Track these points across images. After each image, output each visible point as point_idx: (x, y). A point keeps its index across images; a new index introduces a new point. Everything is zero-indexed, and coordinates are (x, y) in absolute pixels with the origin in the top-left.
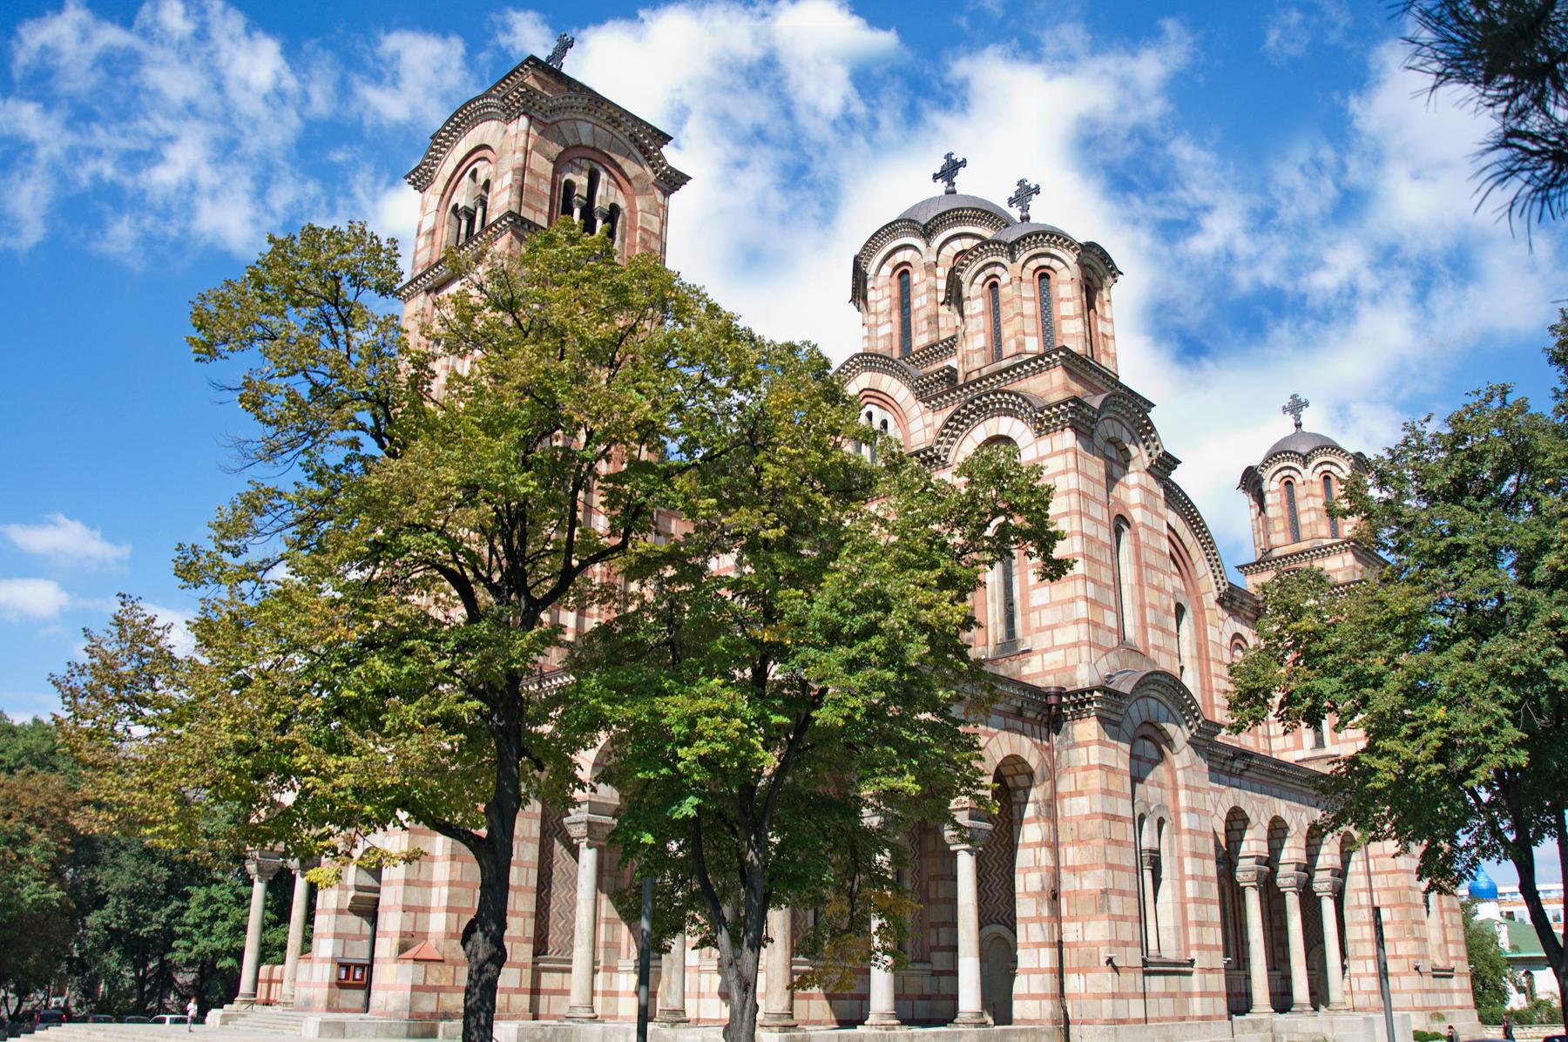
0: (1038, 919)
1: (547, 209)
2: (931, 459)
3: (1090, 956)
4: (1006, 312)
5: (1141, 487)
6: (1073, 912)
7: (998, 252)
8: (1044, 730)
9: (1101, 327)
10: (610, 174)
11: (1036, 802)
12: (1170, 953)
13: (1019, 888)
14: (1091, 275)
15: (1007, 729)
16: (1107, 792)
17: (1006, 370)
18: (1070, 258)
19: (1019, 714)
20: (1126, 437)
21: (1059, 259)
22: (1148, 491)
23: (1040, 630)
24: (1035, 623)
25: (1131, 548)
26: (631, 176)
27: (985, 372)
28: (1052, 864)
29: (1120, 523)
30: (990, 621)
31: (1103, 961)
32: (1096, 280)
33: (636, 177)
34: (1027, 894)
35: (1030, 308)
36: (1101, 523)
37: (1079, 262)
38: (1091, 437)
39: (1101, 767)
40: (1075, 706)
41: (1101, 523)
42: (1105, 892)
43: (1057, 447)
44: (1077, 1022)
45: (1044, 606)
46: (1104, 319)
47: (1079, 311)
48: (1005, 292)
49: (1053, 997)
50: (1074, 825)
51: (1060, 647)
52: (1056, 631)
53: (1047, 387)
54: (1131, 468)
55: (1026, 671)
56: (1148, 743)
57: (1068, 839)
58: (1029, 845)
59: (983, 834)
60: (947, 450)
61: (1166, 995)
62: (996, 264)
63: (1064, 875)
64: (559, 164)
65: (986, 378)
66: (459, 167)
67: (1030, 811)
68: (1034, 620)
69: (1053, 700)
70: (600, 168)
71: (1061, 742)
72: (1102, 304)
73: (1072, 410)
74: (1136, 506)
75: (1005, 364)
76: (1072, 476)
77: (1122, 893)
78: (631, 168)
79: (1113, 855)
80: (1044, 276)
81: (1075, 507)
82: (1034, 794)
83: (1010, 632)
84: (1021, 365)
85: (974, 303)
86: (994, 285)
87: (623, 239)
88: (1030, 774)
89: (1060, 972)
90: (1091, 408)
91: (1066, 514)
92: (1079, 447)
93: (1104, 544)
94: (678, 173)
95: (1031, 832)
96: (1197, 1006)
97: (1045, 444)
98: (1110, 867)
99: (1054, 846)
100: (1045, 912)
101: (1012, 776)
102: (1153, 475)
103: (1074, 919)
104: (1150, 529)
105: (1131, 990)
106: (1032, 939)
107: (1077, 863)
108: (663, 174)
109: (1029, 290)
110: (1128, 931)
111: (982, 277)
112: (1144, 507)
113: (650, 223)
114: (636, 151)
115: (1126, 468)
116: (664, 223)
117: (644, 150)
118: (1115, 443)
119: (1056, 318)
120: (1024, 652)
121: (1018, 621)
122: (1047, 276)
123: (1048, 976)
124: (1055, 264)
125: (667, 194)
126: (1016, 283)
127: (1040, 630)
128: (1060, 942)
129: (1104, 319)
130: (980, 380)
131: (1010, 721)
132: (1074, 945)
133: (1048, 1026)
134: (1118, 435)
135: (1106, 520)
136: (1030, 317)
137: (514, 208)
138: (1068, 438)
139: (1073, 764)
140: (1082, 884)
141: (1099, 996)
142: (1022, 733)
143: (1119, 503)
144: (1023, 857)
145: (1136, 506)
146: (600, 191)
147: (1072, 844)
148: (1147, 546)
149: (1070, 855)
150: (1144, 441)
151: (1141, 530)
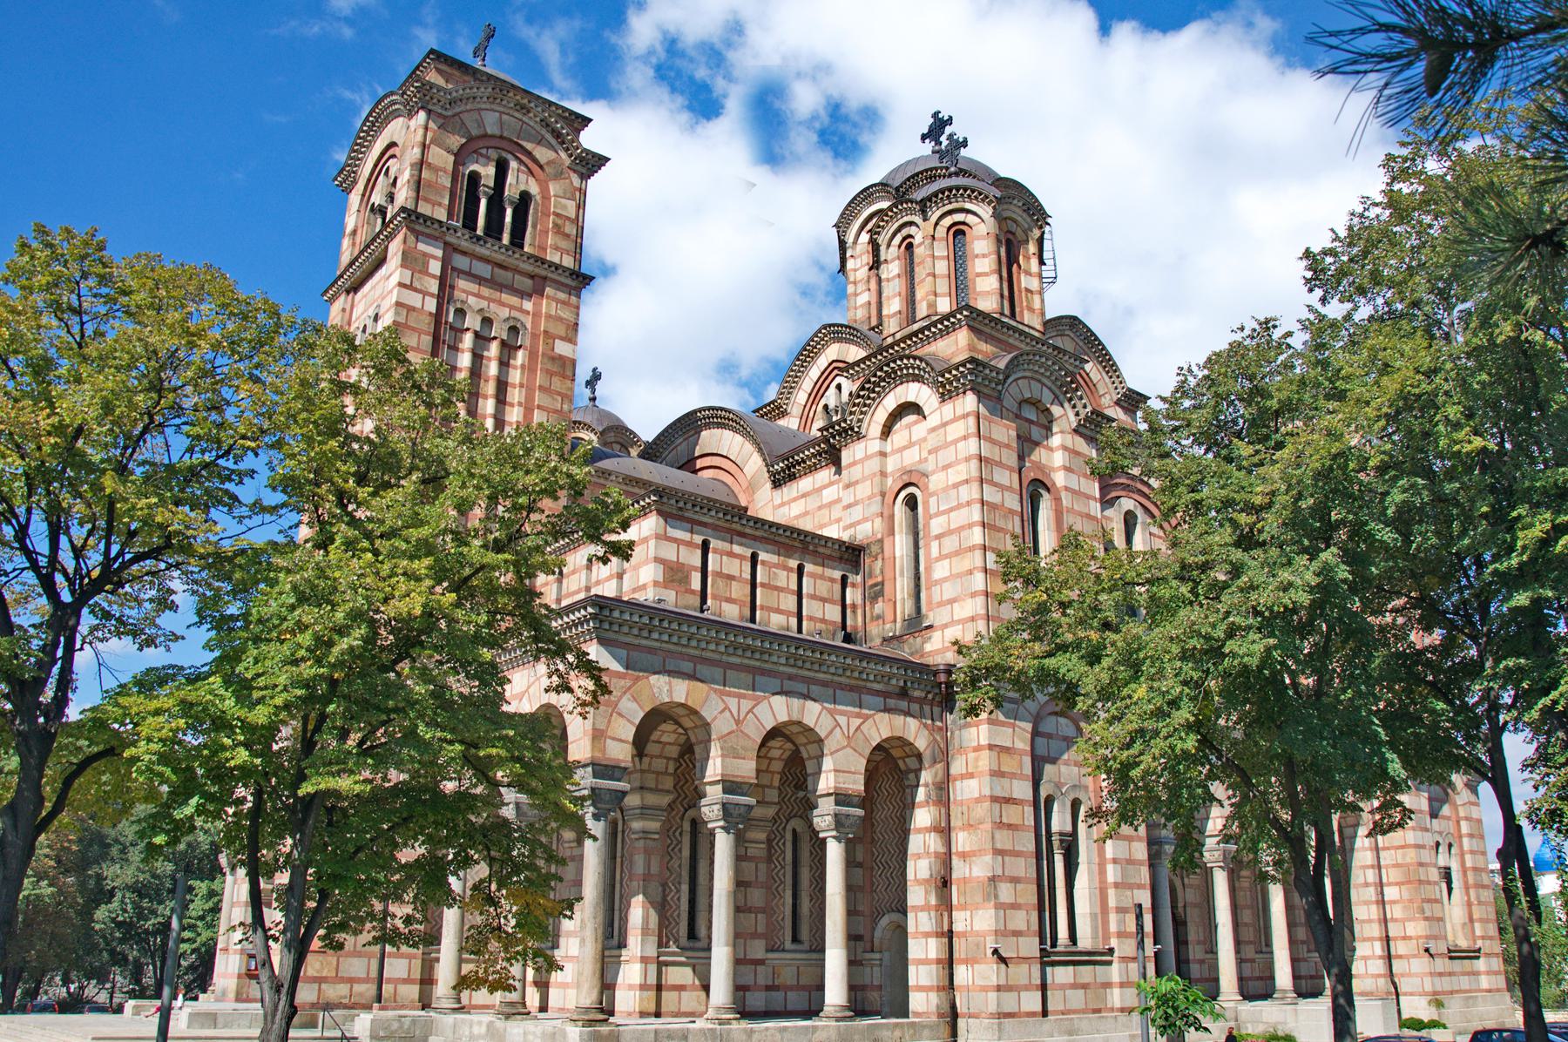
1: (446, 202)
2: (845, 430)
3: (977, 945)
4: (920, 272)
5: (1065, 448)
6: (962, 901)
7: (911, 211)
8: (936, 710)
9: (1025, 282)
10: (521, 161)
11: (926, 785)
12: (1085, 942)
13: (910, 875)
14: (1013, 227)
15: (887, 710)
16: (997, 774)
17: (915, 334)
18: (985, 211)
19: (903, 693)
20: (1047, 397)
21: (975, 214)
22: (1072, 452)
23: (941, 604)
24: (936, 598)
25: (1052, 514)
26: (543, 161)
27: (898, 336)
28: (942, 850)
29: (1035, 490)
30: (899, 597)
31: (989, 952)
32: (1019, 233)
33: (548, 163)
34: (918, 882)
35: (942, 267)
36: (1009, 489)
37: (994, 215)
38: (999, 399)
39: (991, 747)
41: (1009, 489)
42: (993, 879)
43: (959, 412)
45: (945, 580)
46: (1028, 273)
47: (994, 266)
48: (919, 252)
49: (939, 989)
51: (960, 622)
52: (956, 605)
53: (953, 349)
54: (1055, 429)
55: (928, 647)
56: (1062, 720)
57: (959, 823)
58: (919, 831)
59: (852, 819)
60: (860, 421)
61: (1075, 986)
62: (911, 223)
63: (955, 861)
64: (460, 156)
65: (897, 343)
66: (376, 166)
67: (921, 794)
69: (942, 678)
70: (509, 157)
71: (954, 722)
72: (1028, 258)
73: (971, 372)
74: (1059, 469)
75: (916, 327)
76: (973, 442)
77: (1015, 880)
78: (543, 154)
79: (1004, 840)
80: (958, 231)
81: (975, 473)
82: (926, 776)
83: (918, 609)
84: (928, 328)
85: (891, 266)
86: (910, 247)
87: (534, 226)
88: (919, 756)
89: (949, 963)
90: (993, 368)
91: (967, 482)
92: (982, 410)
93: (1011, 511)
94: (594, 155)
95: (923, 817)
96: (1116, 997)
97: (948, 410)
98: (998, 852)
99: (944, 831)
100: (933, 901)
101: (903, 758)
102: (1081, 435)
103: (963, 907)
104: (1075, 493)
105: (1025, 981)
106: (921, 929)
108: (581, 159)
109: (941, 250)
110: (1025, 920)
111: (898, 238)
112: (1068, 469)
113: (565, 207)
114: (549, 136)
115: (1049, 429)
116: (581, 206)
117: (557, 135)
118: (1035, 403)
119: (970, 276)
120: (928, 627)
121: (923, 595)
122: (963, 233)
123: (934, 967)
124: (970, 219)
125: (585, 177)
126: (928, 242)
127: (941, 604)
128: (951, 931)
129: (1028, 273)
130: (891, 346)
131: (892, 702)
132: (964, 934)
133: (934, 1019)
134: (1036, 395)
135: (1016, 485)
136: (942, 276)
137: (410, 206)
138: (969, 402)
139: (965, 744)
140: (972, 871)
141: (984, 989)
142: (908, 713)
143: (1039, 466)
144: (915, 843)
145: (1059, 469)
146: (510, 179)
147: (963, 829)
148: (1070, 510)
149: (961, 840)
150: (1070, 400)
151: (1063, 494)
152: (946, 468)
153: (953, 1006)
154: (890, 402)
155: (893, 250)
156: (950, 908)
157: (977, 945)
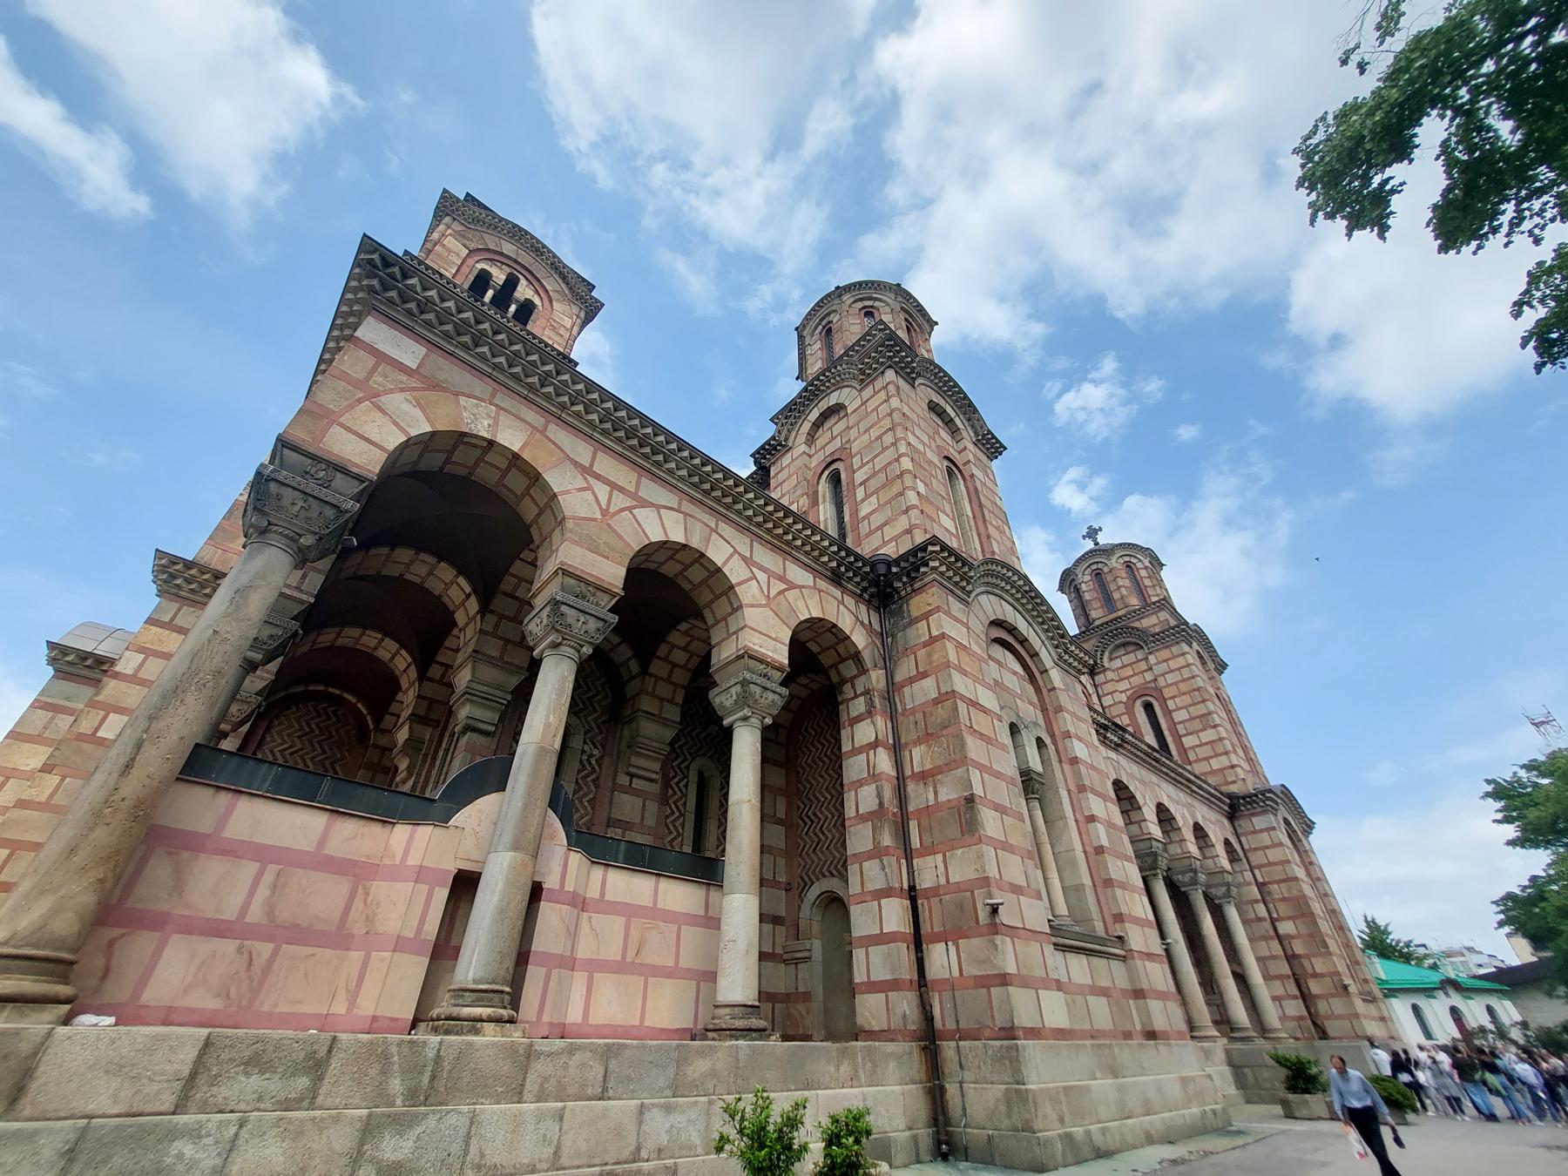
0: (878, 853)
3: (961, 906)
6: (928, 841)
13: (850, 812)
40: (908, 576)
44: (949, 1036)
50: (919, 716)
51: (890, 541)
63: (911, 787)
67: (859, 706)
68: (864, 528)
88: (856, 656)
89: (918, 942)
100: (887, 840)
103: (928, 851)
106: (870, 887)
107: (928, 766)
124: (877, 304)
127: (871, 533)
128: (912, 888)
132: (935, 892)
147: (918, 742)
152: (868, 430)
153: (928, 1018)
154: (814, 415)
155: (816, 337)
156: (908, 854)
157: (961, 906)
